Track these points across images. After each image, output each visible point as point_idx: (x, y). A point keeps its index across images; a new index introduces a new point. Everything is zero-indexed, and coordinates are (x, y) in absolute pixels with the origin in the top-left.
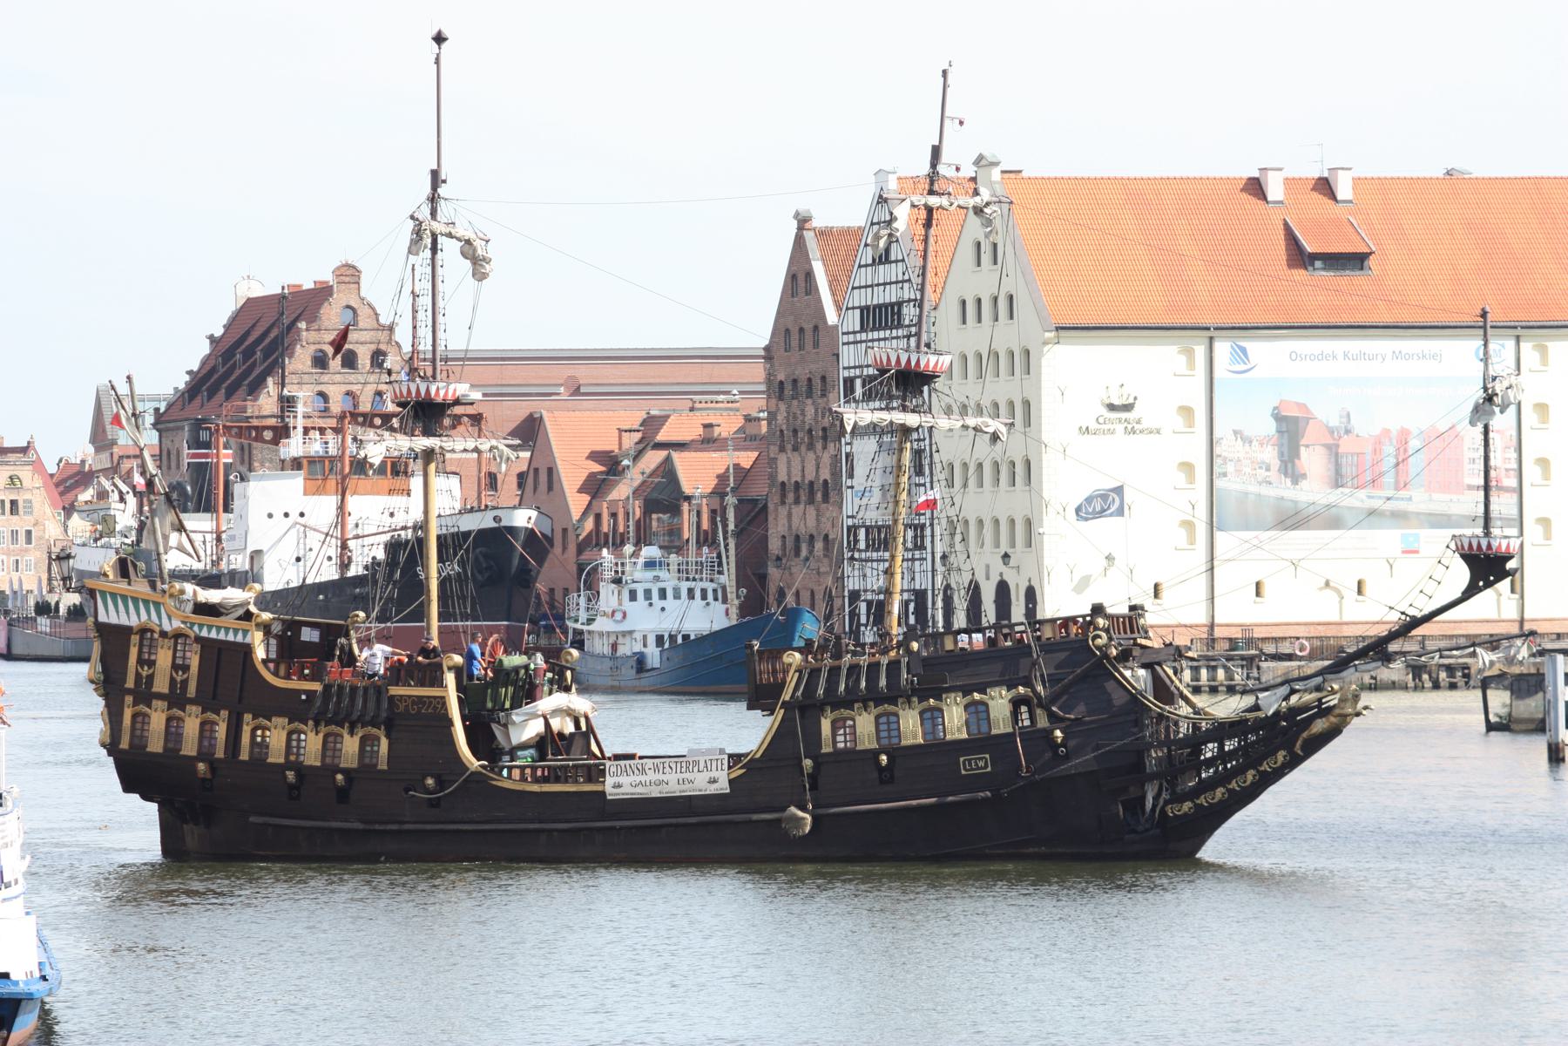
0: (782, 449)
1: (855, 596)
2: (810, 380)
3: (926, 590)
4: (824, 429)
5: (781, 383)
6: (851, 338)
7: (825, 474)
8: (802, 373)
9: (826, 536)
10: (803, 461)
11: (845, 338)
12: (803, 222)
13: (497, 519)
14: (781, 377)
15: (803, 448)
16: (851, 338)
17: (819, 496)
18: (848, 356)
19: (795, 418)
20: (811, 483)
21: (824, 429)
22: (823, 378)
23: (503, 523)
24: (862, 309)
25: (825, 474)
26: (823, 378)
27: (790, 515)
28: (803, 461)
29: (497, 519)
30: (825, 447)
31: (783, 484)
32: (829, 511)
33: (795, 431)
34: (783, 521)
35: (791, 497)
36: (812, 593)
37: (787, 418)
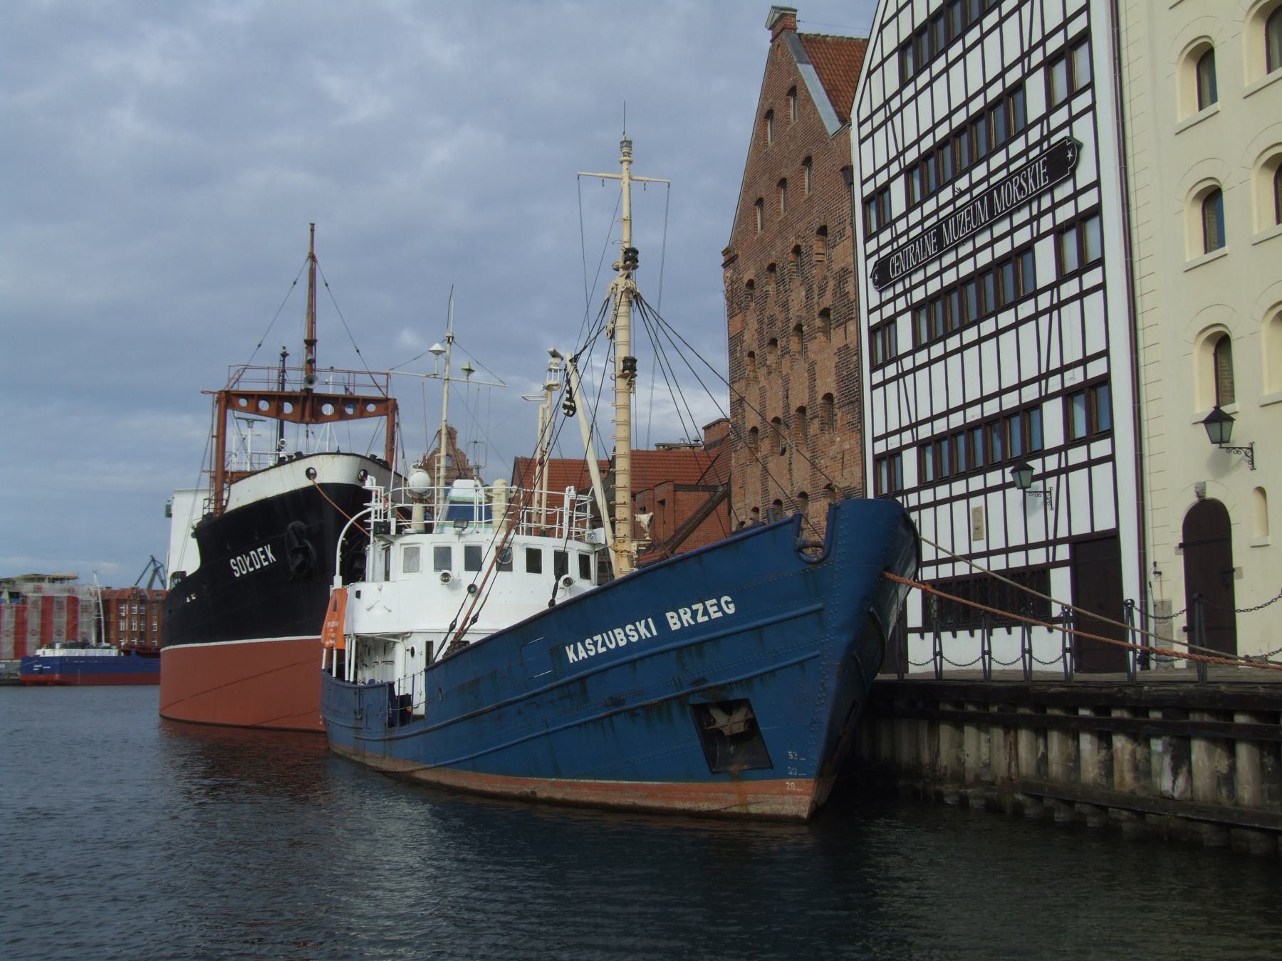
2: (797, 250)
3: (1111, 539)
4: (825, 313)
7: (828, 383)
8: (780, 251)
11: (866, 129)
12: (782, 22)
13: (310, 474)
19: (772, 322)
21: (825, 313)
23: (318, 480)
24: (902, 48)
25: (828, 383)
26: (823, 231)
29: (310, 474)
32: (841, 442)
33: (773, 342)
34: (754, 486)
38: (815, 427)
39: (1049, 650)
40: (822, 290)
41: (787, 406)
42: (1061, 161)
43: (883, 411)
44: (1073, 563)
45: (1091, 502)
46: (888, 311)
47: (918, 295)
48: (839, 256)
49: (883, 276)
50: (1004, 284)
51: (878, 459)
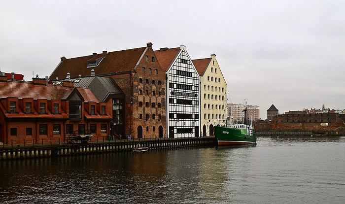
0: (141, 94)
1: (172, 128)
4: (160, 92)
5: (141, 79)
6: (173, 75)
8: (151, 79)
9: (159, 115)
10: (150, 98)
14: (141, 78)
15: (150, 95)
16: (173, 75)
17: (156, 106)
18: (170, 79)
20: (154, 103)
21: (160, 92)
22: (159, 82)
27: (144, 110)
28: (150, 98)
30: (160, 95)
31: (141, 102)
33: (147, 91)
35: (144, 106)
36: (154, 127)
37: (144, 88)
38: (156, 106)
39: (193, 135)
40: (159, 89)
41: (150, 101)
42: (196, 95)
43: (170, 108)
44: (195, 128)
45: (197, 124)
46: (173, 98)
47: (178, 98)
48: (163, 86)
49: (172, 93)
50: (189, 103)
51: (170, 114)
